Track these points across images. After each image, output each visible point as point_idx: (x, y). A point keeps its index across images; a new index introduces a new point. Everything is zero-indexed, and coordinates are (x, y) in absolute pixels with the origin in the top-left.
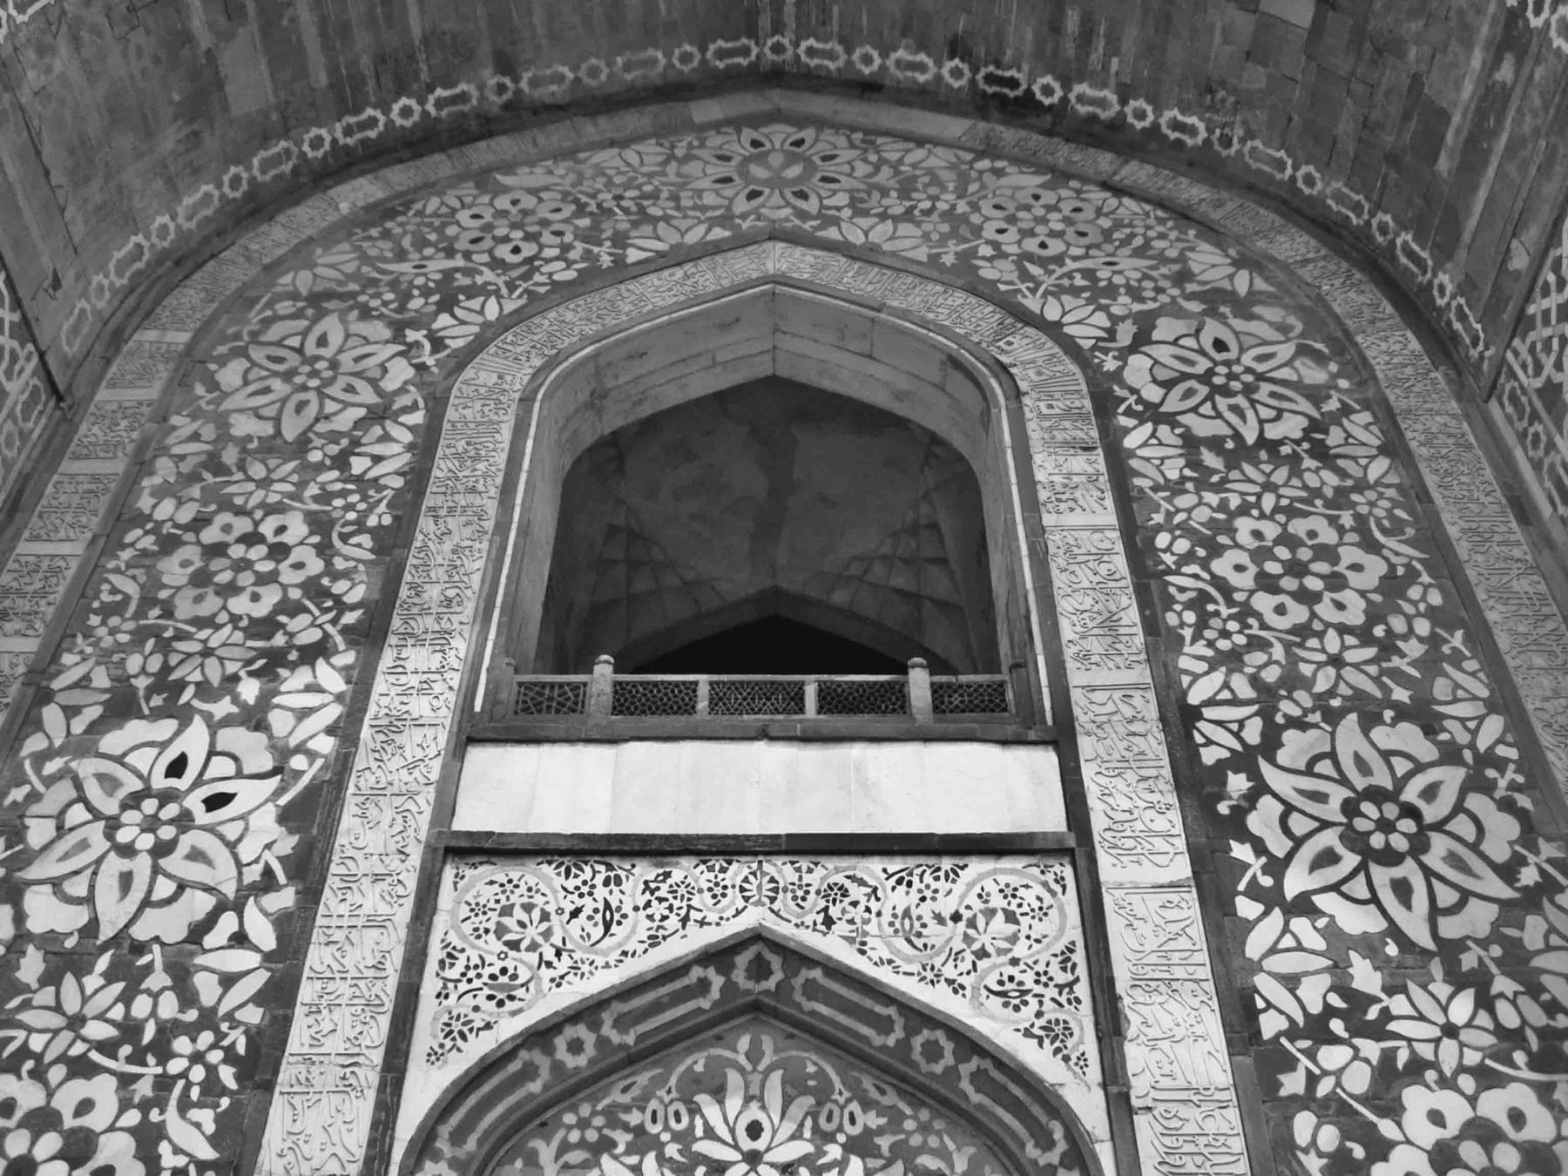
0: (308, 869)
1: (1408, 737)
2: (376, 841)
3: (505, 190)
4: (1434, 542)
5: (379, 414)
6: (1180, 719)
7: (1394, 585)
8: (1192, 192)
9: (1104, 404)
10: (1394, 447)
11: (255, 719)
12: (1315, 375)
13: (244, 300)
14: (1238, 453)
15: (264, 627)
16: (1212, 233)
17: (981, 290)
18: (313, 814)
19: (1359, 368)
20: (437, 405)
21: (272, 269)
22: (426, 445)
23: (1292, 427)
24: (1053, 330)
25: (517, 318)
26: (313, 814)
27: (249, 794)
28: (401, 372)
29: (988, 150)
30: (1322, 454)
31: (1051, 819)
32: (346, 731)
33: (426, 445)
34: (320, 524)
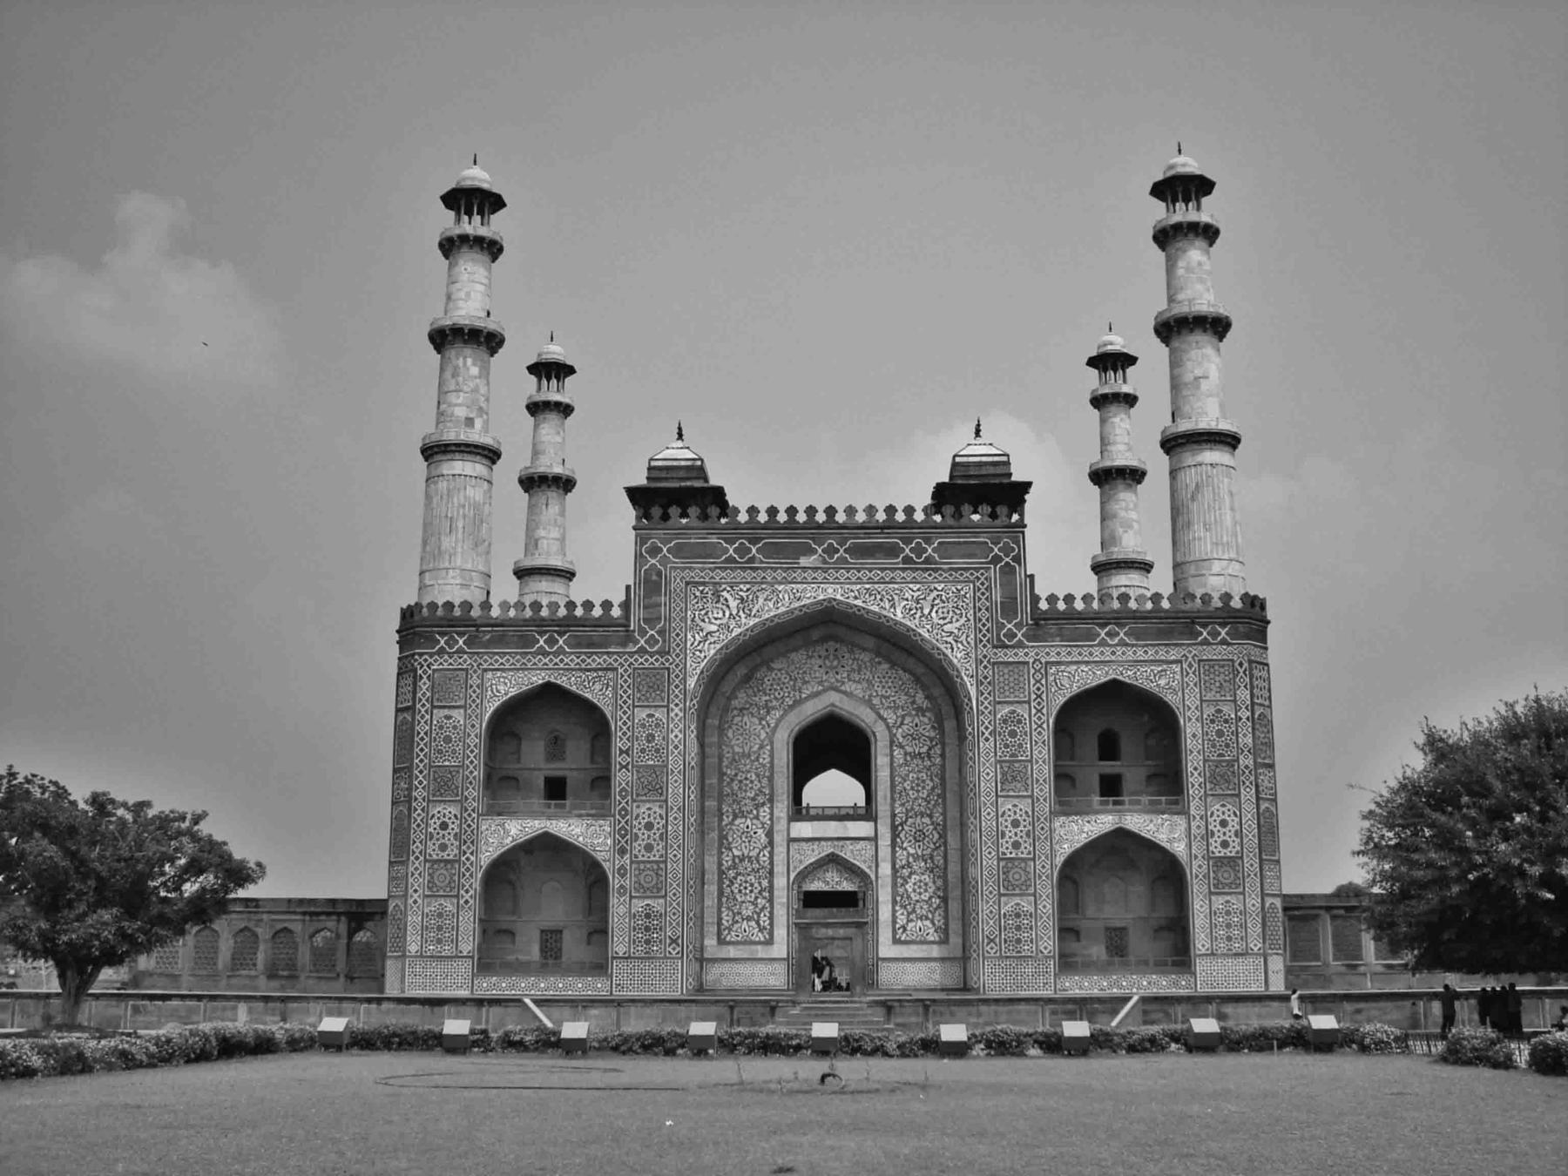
0: (771, 843)
1: (927, 820)
2: (779, 839)
3: (772, 670)
4: (943, 779)
5: (761, 747)
6: (894, 816)
7: (933, 789)
8: (920, 670)
9: (892, 742)
10: (943, 756)
11: (757, 817)
12: (933, 734)
13: (726, 709)
14: (915, 756)
15: (753, 799)
16: (924, 688)
17: (872, 707)
18: (770, 834)
19: (942, 732)
20: (772, 743)
21: (729, 699)
22: (772, 756)
23: (924, 750)
24: (884, 720)
25: (782, 717)
26: (770, 834)
27: (760, 831)
28: (763, 735)
29: (878, 654)
30: (929, 757)
31: (872, 834)
32: (771, 819)
33: (772, 756)
34: (758, 775)
